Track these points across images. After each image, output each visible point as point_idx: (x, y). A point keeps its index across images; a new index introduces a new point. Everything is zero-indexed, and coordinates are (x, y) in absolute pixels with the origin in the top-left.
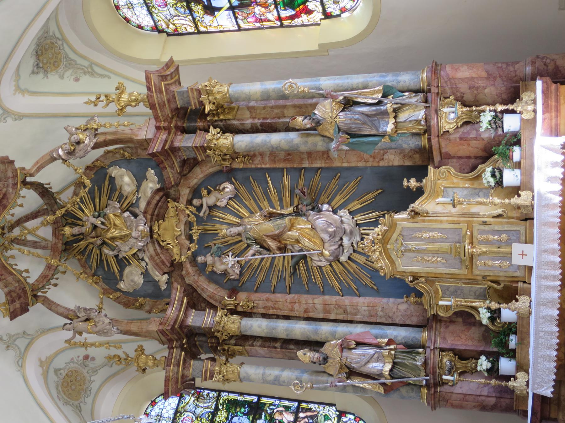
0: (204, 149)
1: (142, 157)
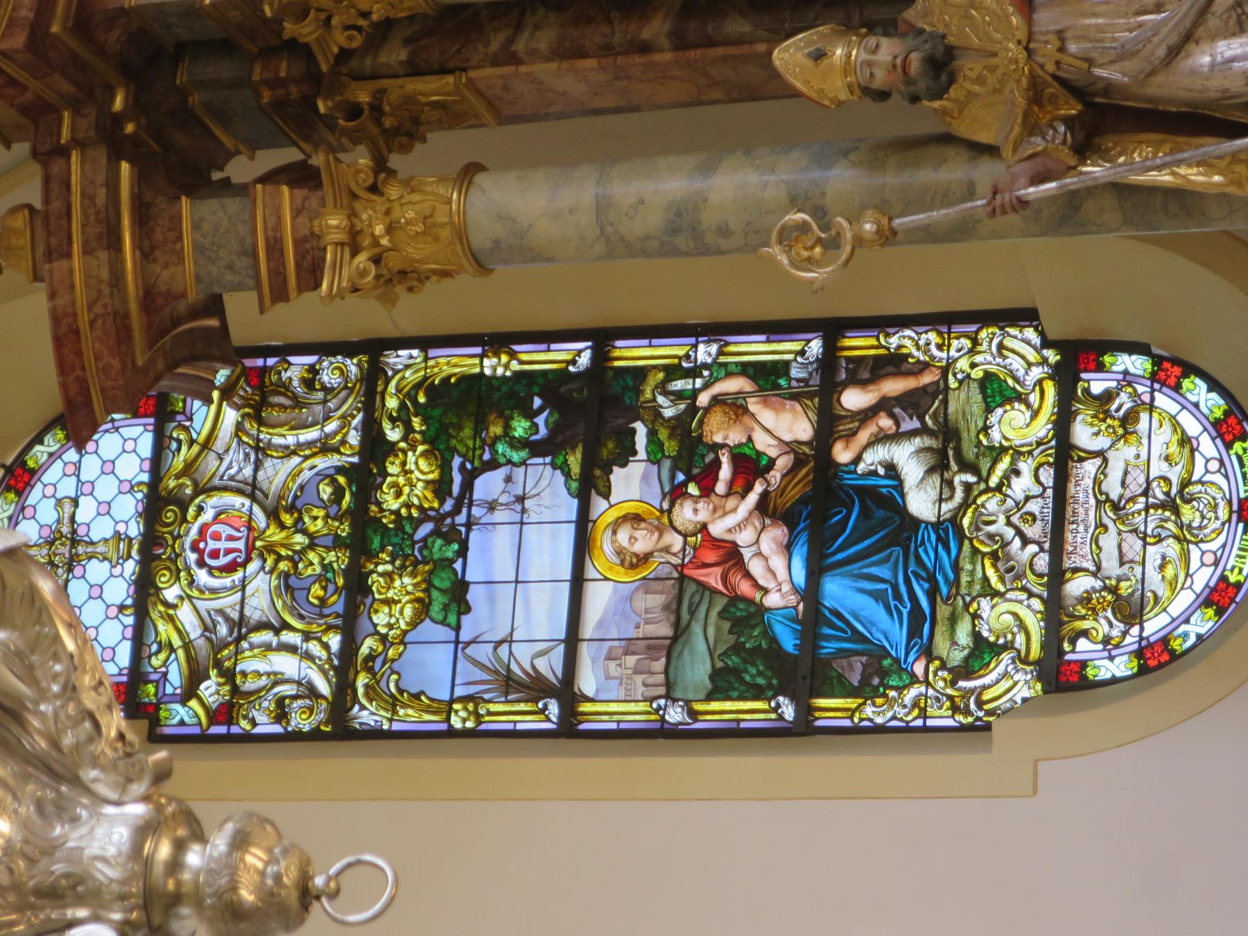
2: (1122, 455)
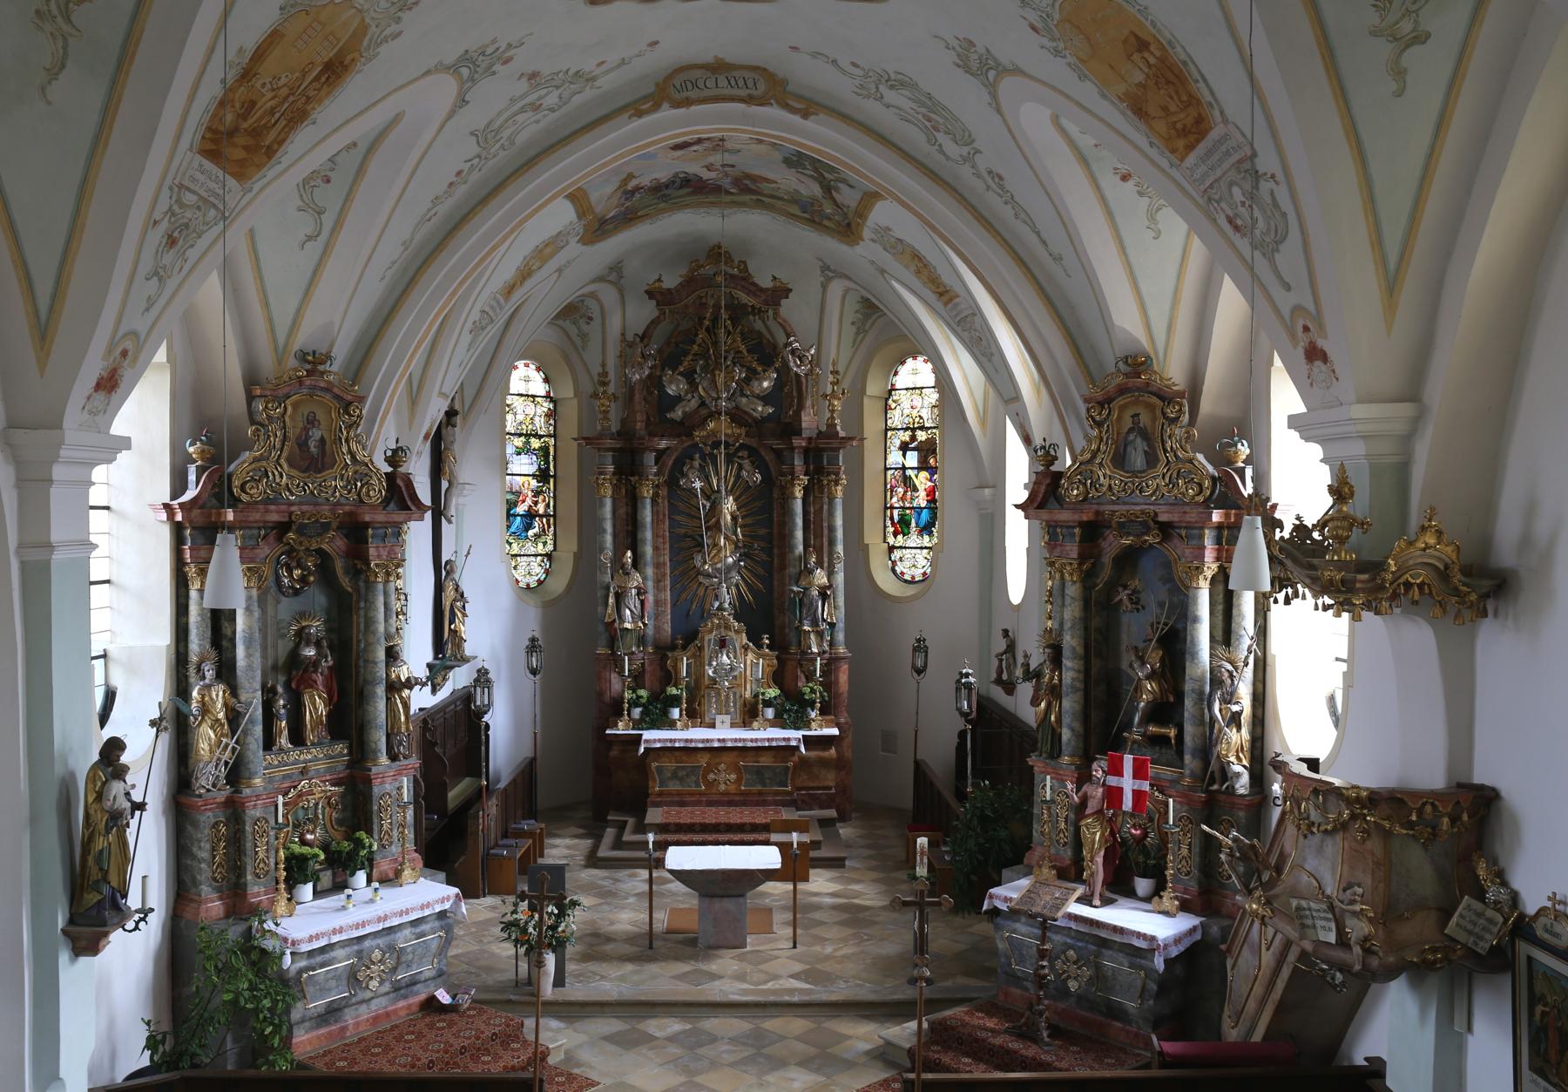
0: (792, 474)
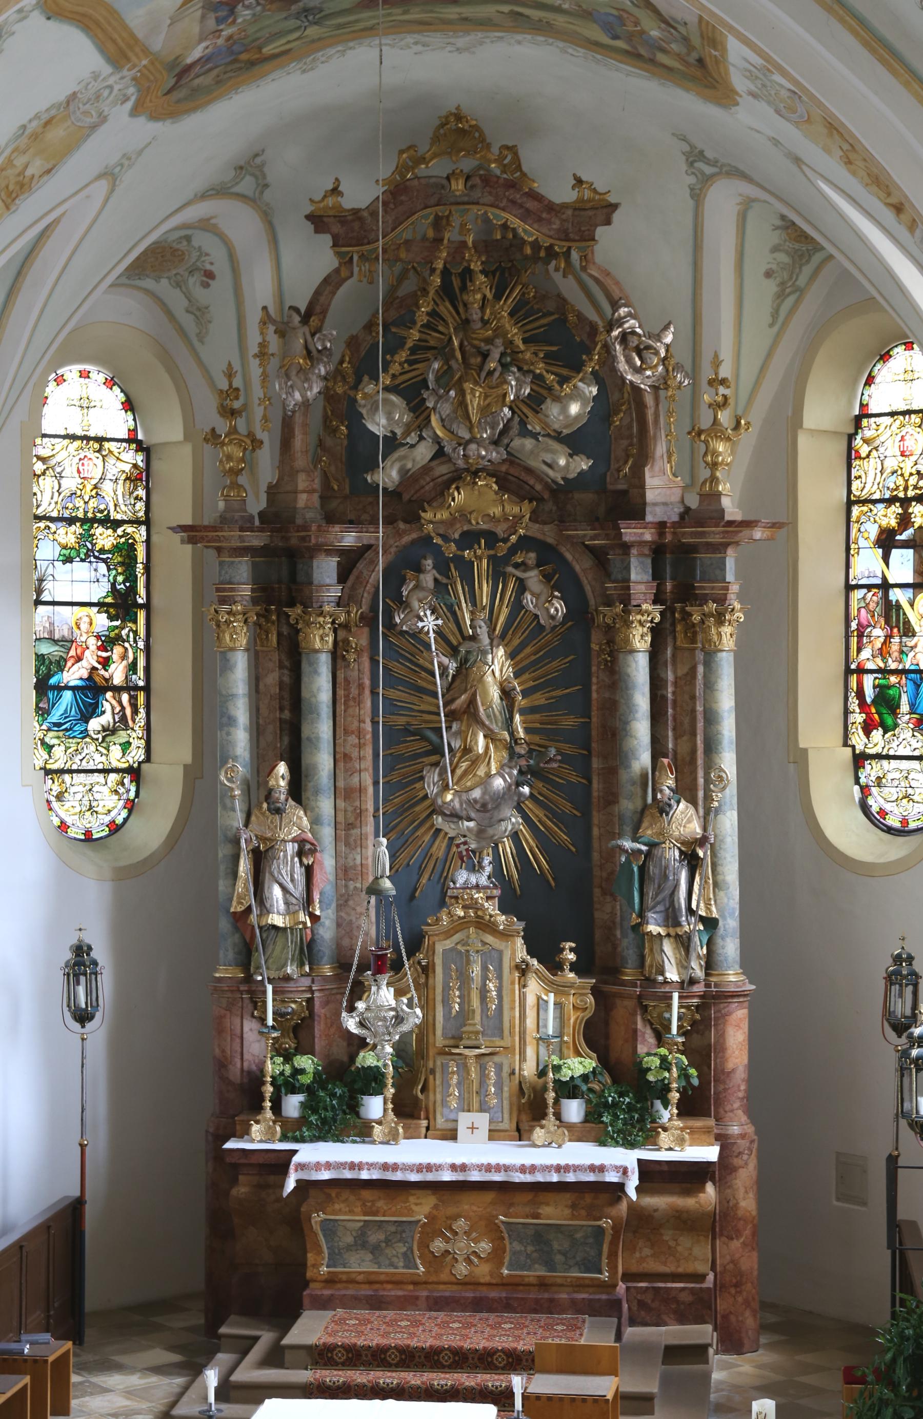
0: (626, 599)
1: (613, 447)
2: (105, 790)
